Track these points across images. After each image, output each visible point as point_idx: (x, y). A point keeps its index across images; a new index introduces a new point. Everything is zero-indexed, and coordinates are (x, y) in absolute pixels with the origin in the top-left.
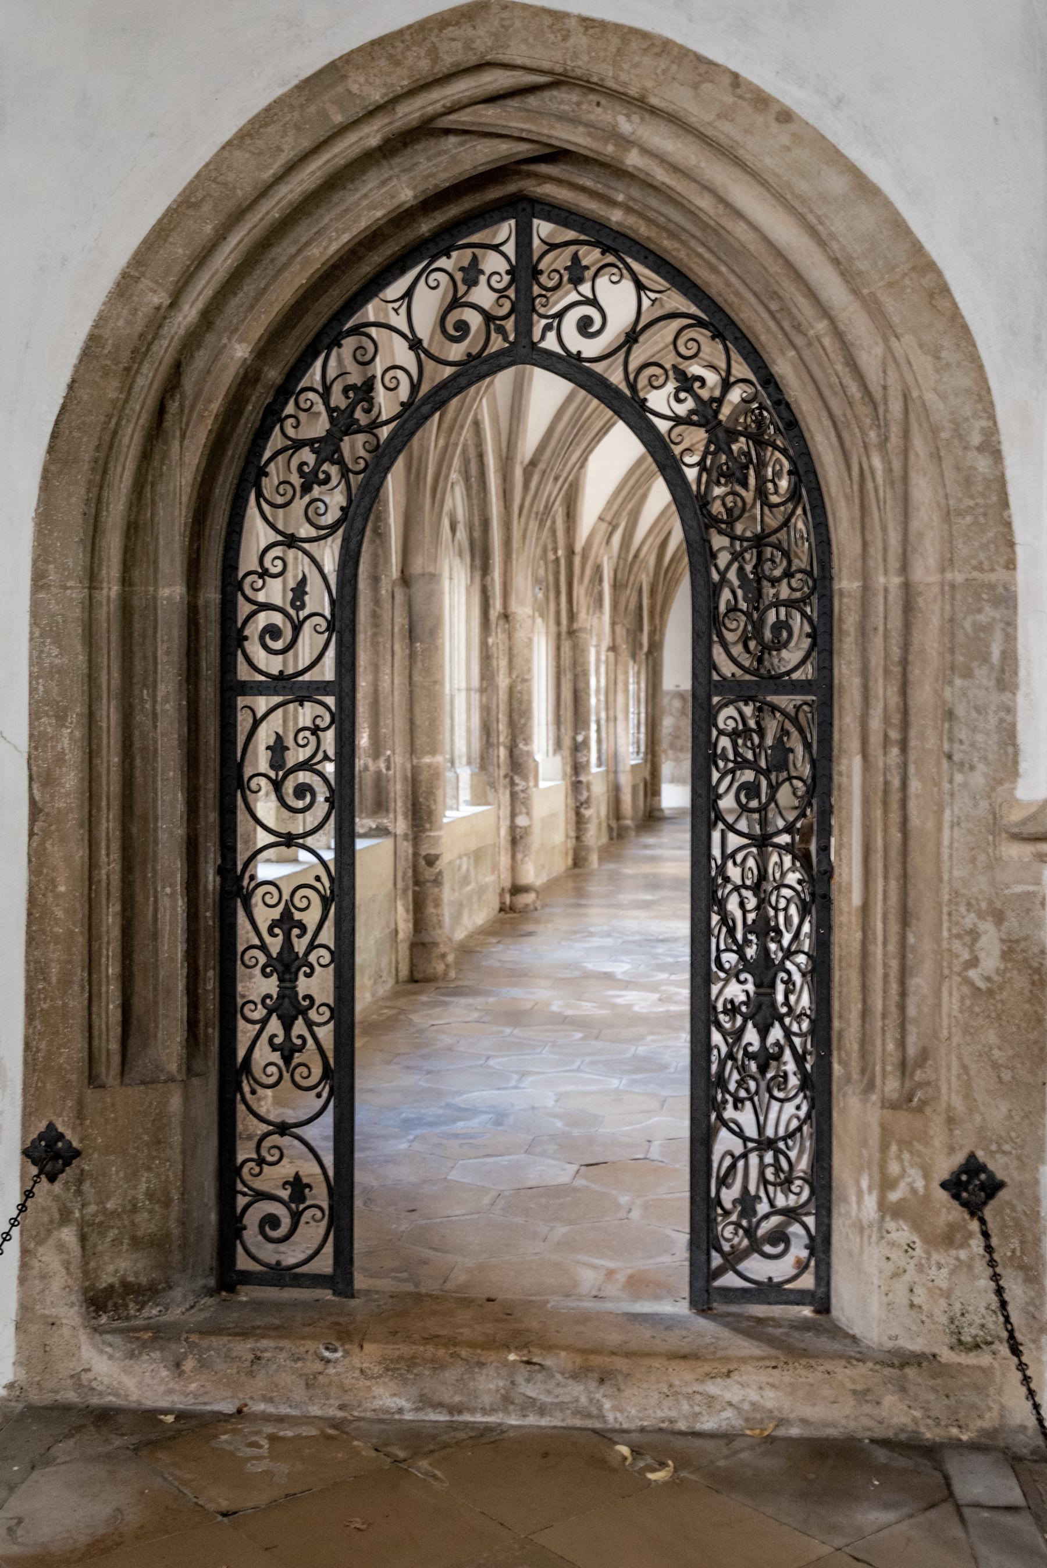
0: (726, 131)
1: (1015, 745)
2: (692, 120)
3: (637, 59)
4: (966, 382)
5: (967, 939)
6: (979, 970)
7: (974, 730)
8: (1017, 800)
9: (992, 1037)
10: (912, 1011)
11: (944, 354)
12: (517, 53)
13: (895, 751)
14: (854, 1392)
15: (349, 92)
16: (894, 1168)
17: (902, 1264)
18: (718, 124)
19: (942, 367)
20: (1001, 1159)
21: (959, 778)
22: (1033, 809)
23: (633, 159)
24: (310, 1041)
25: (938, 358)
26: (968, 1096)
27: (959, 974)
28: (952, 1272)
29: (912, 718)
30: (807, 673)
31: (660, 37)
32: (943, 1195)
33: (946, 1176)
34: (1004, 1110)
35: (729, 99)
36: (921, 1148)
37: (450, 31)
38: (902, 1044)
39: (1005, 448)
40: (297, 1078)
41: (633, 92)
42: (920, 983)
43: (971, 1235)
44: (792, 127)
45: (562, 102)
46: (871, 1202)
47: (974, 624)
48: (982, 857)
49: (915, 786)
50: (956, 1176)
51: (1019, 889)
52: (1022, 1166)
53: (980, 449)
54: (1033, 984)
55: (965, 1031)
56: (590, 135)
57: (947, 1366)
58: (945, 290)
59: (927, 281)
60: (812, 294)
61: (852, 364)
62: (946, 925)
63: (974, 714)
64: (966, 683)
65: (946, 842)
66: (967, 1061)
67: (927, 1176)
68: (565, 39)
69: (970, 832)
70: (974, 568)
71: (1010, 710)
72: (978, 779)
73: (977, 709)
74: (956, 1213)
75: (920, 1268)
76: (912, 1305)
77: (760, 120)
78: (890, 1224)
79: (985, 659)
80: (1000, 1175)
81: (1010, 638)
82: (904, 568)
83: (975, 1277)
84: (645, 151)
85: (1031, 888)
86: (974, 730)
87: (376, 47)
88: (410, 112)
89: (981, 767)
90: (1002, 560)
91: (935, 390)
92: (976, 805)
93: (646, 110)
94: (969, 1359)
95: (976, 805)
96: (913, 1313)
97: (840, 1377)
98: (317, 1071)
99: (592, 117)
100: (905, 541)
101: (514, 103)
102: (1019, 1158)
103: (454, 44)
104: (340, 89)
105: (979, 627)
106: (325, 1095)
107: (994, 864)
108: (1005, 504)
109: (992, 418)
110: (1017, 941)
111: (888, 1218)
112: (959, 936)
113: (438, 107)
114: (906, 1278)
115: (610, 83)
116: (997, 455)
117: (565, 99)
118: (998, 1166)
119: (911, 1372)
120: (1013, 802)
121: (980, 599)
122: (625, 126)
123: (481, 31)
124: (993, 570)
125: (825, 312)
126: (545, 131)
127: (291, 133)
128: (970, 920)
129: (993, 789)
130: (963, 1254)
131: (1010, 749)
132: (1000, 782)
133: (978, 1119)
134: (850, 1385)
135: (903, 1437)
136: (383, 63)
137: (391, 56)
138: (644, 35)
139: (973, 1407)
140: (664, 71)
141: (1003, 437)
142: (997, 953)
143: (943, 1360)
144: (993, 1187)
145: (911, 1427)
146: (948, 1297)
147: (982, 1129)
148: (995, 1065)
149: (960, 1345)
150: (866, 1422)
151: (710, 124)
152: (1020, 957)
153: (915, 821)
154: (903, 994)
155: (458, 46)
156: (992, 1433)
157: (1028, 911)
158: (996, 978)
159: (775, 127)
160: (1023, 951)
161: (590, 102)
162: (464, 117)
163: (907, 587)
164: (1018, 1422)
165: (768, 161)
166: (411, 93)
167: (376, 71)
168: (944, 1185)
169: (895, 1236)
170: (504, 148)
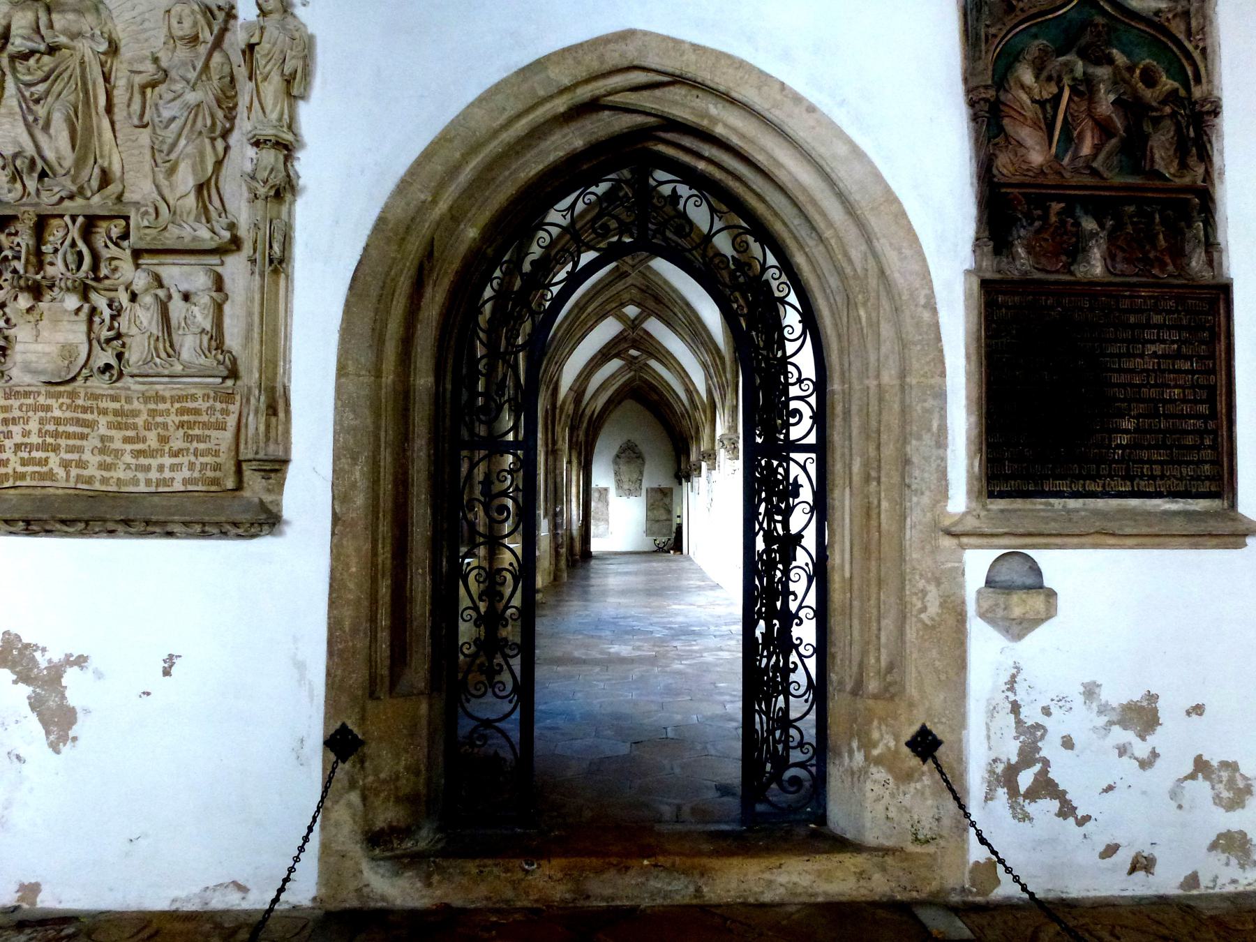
0: (776, 115)
1: (946, 480)
2: (757, 107)
3: (725, 70)
4: (916, 267)
5: (920, 595)
6: (927, 614)
7: (923, 471)
8: (948, 513)
9: (934, 653)
10: (883, 640)
11: (903, 250)
12: (652, 61)
13: (875, 483)
14: (855, 873)
15: (548, 77)
16: (875, 735)
17: (881, 793)
18: (773, 110)
19: (903, 258)
20: (941, 727)
21: (915, 499)
22: (956, 518)
23: (719, 130)
24: (505, 667)
25: (901, 253)
26: (921, 690)
27: (916, 617)
28: (913, 797)
29: (882, 464)
30: (812, 439)
31: (738, 58)
32: (906, 750)
33: (908, 738)
34: (942, 697)
35: (779, 97)
36: (892, 722)
37: (611, 46)
38: (878, 660)
39: (939, 306)
40: (497, 690)
41: (722, 88)
42: (888, 623)
43: (923, 774)
44: (815, 115)
45: (675, 94)
46: (859, 757)
47: (922, 407)
48: (928, 547)
49: (885, 505)
50: (914, 738)
51: (949, 565)
52: (953, 731)
53: (925, 306)
54: (958, 621)
55: (919, 651)
56: (692, 113)
57: (911, 854)
58: (903, 214)
59: (894, 208)
60: (824, 215)
61: (846, 255)
62: (907, 587)
63: (923, 462)
64: (918, 443)
65: (908, 537)
66: (920, 668)
67: (897, 738)
68: (681, 55)
69: (921, 531)
70: (923, 376)
71: (943, 459)
72: (926, 500)
73: (924, 458)
74: (915, 761)
75: (892, 795)
76: (887, 818)
77: (796, 111)
78: (873, 769)
79: (929, 430)
80: (940, 737)
81: (943, 418)
82: (878, 376)
83: (926, 799)
84: (726, 125)
85: (956, 565)
86: (923, 471)
87: (566, 53)
88: (584, 93)
89: (927, 493)
90: (938, 373)
91: (899, 272)
92: (925, 516)
93: (728, 101)
95: (925, 516)
96: (889, 824)
97: (847, 864)
98: (509, 687)
99: (693, 104)
100: (878, 360)
101: (646, 93)
102: (950, 727)
103: (613, 53)
104: (542, 76)
105: (926, 411)
106: (514, 701)
107: (936, 549)
108: (938, 339)
109: (931, 289)
110: (948, 597)
111: (872, 765)
112: (916, 594)
113: (602, 91)
114: (884, 802)
115: (709, 83)
116: (934, 311)
117: (677, 92)
118: (938, 731)
119: (889, 860)
121: (926, 394)
122: (713, 110)
123: (631, 47)
124: (932, 377)
125: (830, 225)
126: (666, 110)
127: (512, 99)
128: (921, 584)
129: (934, 506)
130: (919, 786)
131: (943, 483)
132: (938, 502)
133: (927, 703)
134: (853, 869)
135: (885, 899)
136: (570, 61)
137: (575, 58)
138: (728, 57)
139: (925, 879)
140: (741, 78)
141: (937, 300)
142: (937, 603)
143: (907, 851)
144: (937, 743)
145: (889, 893)
146: (910, 812)
147: (929, 709)
148: (937, 671)
149: (917, 840)
150: (863, 891)
151: (768, 110)
152: (951, 606)
153: (884, 526)
154: (879, 630)
155: (617, 55)
156: (935, 894)
157: (955, 578)
158: (937, 618)
159: (805, 115)
160: (952, 602)
161: (692, 95)
162: (617, 98)
163: (879, 385)
164: (951, 886)
165: (801, 134)
166: (587, 81)
167: (566, 66)
168: (908, 744)
169: (877, 776)
170: (639, 119)
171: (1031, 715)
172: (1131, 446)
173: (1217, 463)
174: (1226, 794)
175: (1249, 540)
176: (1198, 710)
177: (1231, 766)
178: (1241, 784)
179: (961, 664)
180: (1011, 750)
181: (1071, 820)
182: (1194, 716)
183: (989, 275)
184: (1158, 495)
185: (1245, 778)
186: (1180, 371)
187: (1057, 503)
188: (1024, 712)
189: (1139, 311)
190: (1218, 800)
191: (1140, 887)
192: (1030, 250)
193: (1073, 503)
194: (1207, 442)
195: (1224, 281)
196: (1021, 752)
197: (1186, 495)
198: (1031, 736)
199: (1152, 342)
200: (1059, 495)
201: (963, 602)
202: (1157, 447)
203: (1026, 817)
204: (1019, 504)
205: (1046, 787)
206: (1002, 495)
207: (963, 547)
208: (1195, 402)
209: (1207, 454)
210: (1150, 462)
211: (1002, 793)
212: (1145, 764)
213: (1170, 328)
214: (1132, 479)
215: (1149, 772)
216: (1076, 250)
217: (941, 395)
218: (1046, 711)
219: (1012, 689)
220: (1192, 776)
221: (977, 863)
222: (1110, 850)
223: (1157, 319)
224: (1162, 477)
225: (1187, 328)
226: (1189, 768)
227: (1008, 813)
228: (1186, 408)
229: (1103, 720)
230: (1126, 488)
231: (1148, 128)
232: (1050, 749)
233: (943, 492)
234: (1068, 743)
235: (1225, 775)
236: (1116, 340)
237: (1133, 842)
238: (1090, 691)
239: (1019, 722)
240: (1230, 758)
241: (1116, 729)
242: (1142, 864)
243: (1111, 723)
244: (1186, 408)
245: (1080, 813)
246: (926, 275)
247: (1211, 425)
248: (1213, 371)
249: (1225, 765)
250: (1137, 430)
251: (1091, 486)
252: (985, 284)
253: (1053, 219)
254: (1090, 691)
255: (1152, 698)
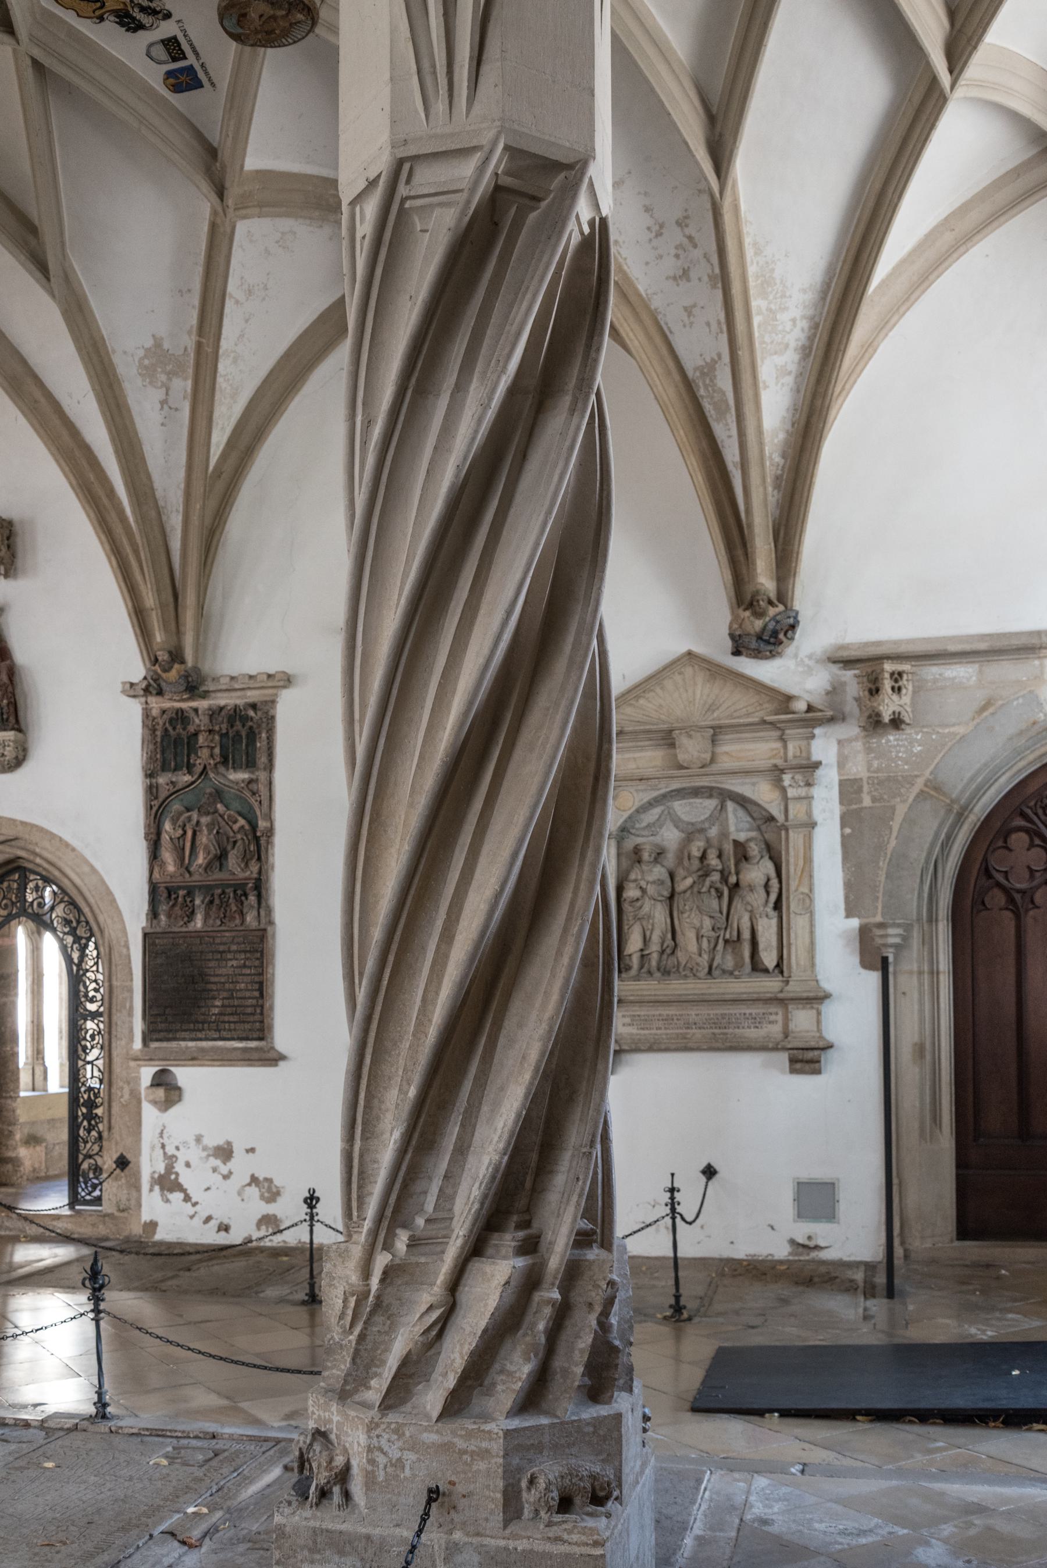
9: (127, 1118)
26: (121, 1136)
72: (123, 1043)
79: (125, 1007)
94: (121, 1214)
108: (130, 962)
116: (128, 948)
118: (129, 1156)
120: (131, 1048)
128: (121, 1084)
171: (170, 1150)
172: (221, 1014)
173: (262, 1022)
174: (266, 1195)
175: (281, 1063)
176: (252, 1150)
177: (270, 1181)
178: (274, 1190)
179: (139, 1123)
180: (161, 1168)
181: (189, 1204)
182: (251, 1154)
183: (148, 931)
184: (233, 1039)
185: (276, 1187)
186: (244, 975)
187: (183, 1044)
188: (167, 1149)
189: (225, 944)
190: (262, 1197)
191: (222, 1239)
192: (169, 916)
193: (191, 1044)
194: (258, 1011)
195: (262, 926)
196: (166, 1168)
197: (247, 1039)
198: (170, 1160)
199: (231, 960)
200: (184, 1039)
201: (140, 1093)
202: (232, 1014)
203: (167, 1201)
204: (165, 1044)
205: (177, 1187)
206: (157, 1040)
207: (140, 1066)
208: (252, 990)
209: (257, 1017)
210: (229, 1022)
211: (157, 1188)
212: (226, 1177)
213: (240, 952)
214: (219, 1031)
215: (228, 1181)
216: (191, 915)
217: (130, 990)
218: (177, 1148)
219: (161, 1137)
220: (249, 1185)
221: (145, 1223)
222: (208, 1219)
223: (234, 948)
224: (235, 1030)
225: (250, 952)
226: (248, 1180)
227: (160, 1198)
228: (248, 994)
229: (205, 1154)
230: (216, 1036)
231: (229, 848)
232: (179, 1167)
233: (131, 1039)
234: (188, 1165)
235: (266, 1185)
236: (213, 959)
237: (221, 1215)
238: (198, 1139)
239: (165, 1153)
240: (268, 1176)
241: (212, 1159)
242: (225, 1228)
243: (209, 1156)
244: (248, 994)
245: (194, 1200)
246: (124, 931)
247: (260, 1002)
248: (262, 974)
249: (266, 1179)
250: (223, 1006)
251: (200, 1035)
252: (146, 935)
253: (180, 899)
254: (198, 1139)
255: (229, 1143)
